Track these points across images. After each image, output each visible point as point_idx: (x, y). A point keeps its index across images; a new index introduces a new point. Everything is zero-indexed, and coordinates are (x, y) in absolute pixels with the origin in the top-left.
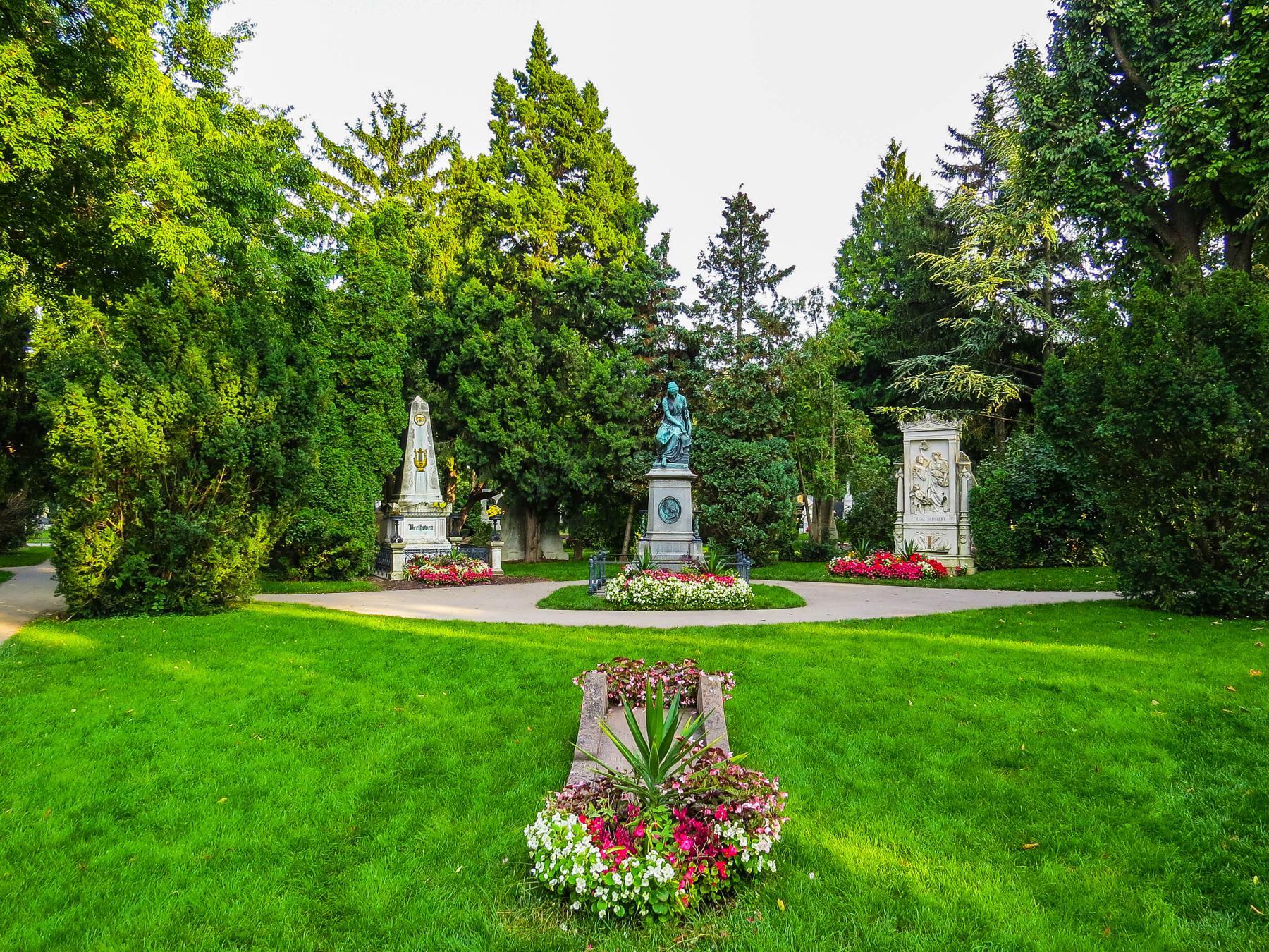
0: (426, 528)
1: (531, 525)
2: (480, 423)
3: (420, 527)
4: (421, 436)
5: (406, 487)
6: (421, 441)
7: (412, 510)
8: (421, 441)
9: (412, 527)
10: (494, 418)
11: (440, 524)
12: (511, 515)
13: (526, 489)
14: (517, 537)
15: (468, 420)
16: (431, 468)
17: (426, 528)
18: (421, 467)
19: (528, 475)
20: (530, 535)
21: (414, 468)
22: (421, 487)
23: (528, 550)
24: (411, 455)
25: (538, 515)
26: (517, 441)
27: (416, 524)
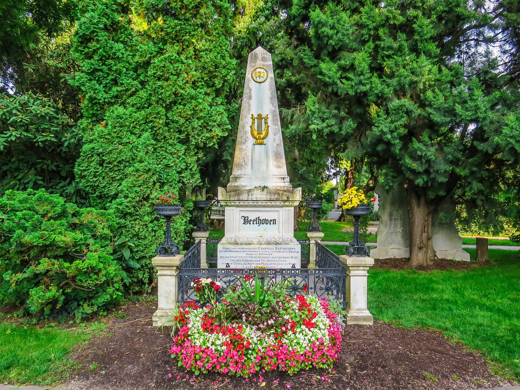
0: (266, 222)
1: (419, 214)
2: (343, 69)
3: (260, 221)
4: (260, 95)
5: (240, 166)
6: (260, 103)
7: (244, 197)
8: (260, 103)
9: (246, 221)
10: (361, 58)
11: (285, 217)
12: (393, 204)
13: (415, 166)
14: (399, 229)
15: (323, 66)
16: (275, 138)
17: (266, 222)
18: (260, 141)
19: (416, 145)
20: (418, 229)
21: (251, 141)
22: (261, 164)
23: (416, 249)
24: (246, 123)
25: (429, 203)
26: (400, 92)
27: (252, 216)
